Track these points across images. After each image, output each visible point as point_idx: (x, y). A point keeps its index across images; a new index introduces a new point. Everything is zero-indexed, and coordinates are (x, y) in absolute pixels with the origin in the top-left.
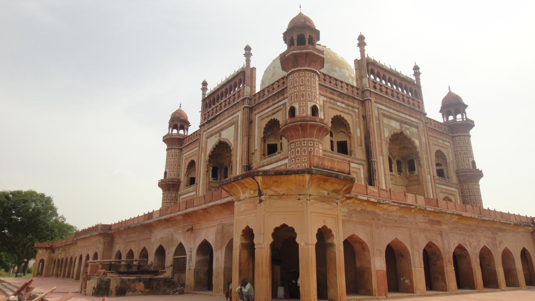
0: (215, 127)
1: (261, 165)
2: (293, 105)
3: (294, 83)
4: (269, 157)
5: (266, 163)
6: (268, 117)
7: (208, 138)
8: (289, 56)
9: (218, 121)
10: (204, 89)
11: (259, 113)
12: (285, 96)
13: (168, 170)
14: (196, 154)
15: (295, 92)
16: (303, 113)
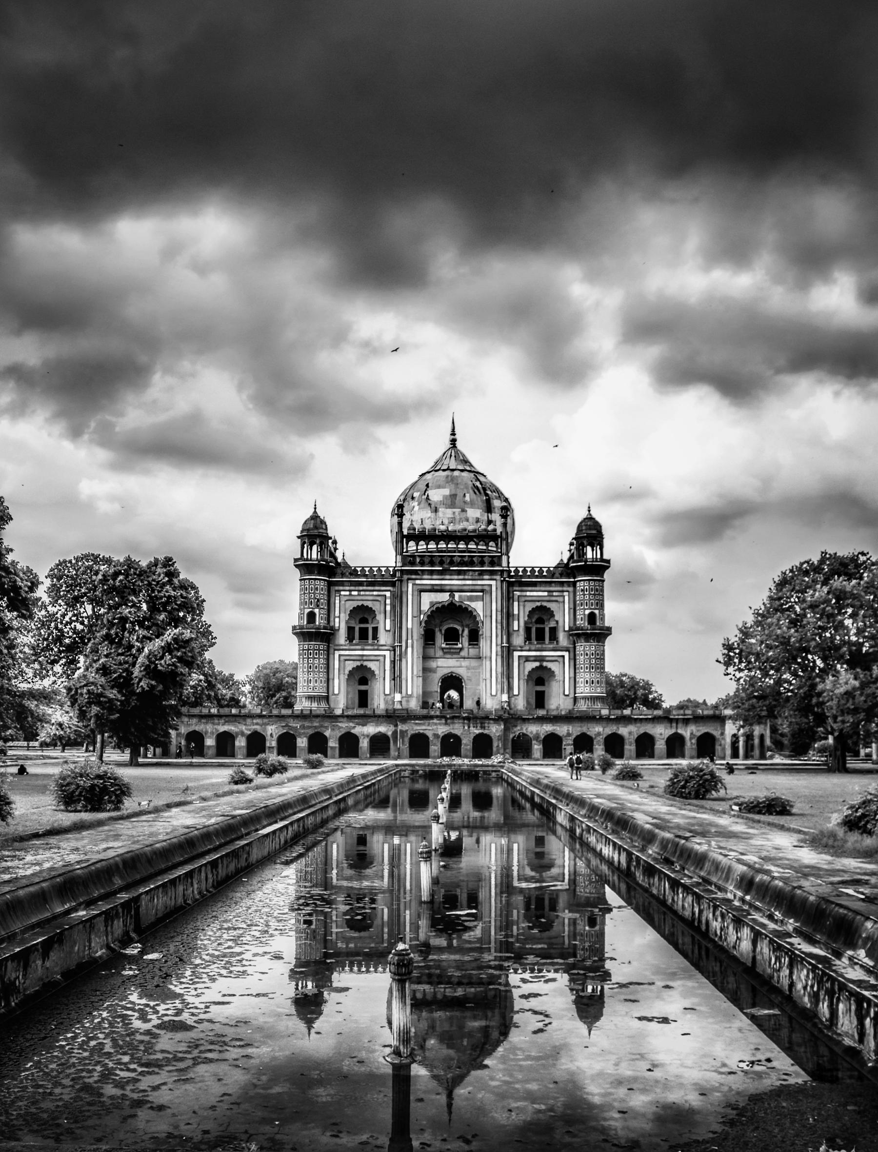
9: (448, 577)
13: (317, 611)
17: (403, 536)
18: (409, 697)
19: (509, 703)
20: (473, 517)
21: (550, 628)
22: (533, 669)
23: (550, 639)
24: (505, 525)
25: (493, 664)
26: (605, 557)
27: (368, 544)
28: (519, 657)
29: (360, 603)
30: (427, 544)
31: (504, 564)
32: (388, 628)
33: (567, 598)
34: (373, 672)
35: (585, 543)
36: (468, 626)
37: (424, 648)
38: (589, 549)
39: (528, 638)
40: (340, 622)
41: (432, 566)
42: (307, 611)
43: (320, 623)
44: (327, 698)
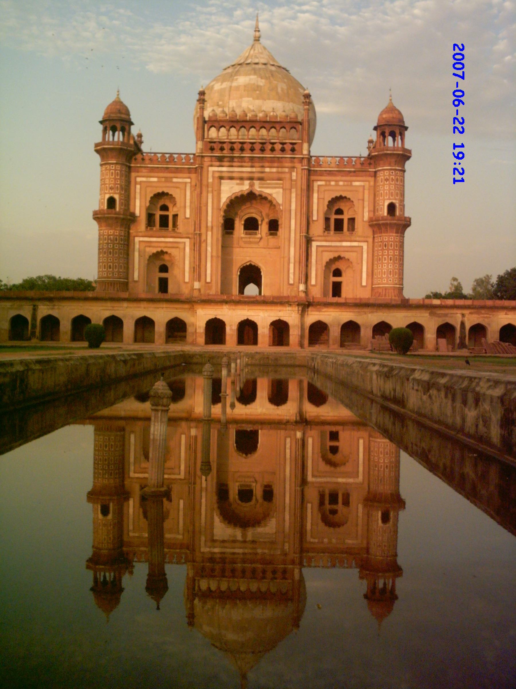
2: (394, 201)
7: (221, 178)
13: (117, 197)
17: (205, 122)
19: (306, 292)
20: (276, 107)
21: (349, 219)
23: (348, 230)
25: (293, 252)
26: (407, 146)
28: (317, 246)
31: (305, 152)
32: (188, 215)
36: (268, 215)
37: (223, 236)
38: (390, 139)
39: (327, 228)
41: (233, 154)
42: (107, 196)
43: (120, 209)
44: (127, 284)
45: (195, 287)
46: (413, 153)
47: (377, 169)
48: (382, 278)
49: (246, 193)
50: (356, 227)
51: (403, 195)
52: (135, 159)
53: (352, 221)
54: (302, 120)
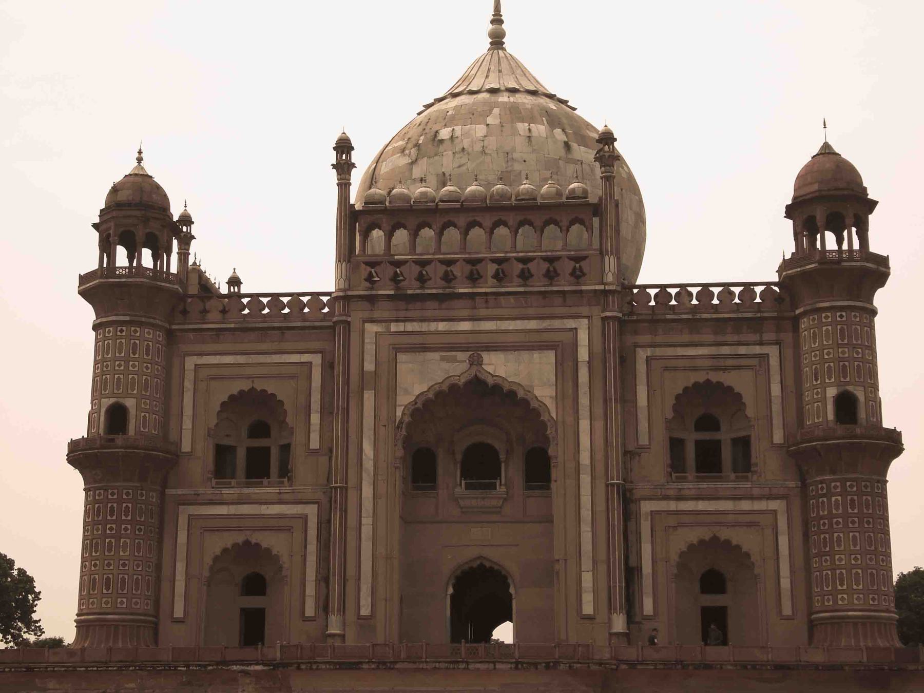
0: (442, 326)
1: (671, 493)
2: (850, 388)
3: (850, 337)
4: (700, 479)
5: (693, 492)
6: (695, 369)
7: (398, 349)
8: (852, 269)
10: (344, 168)
11: (653, 345)
12: (769, 336)
13: (130, 403)
14: (292, 377)
15: (856, 359)
16: (873, 417)
18: (365, 624)
21: (735, 441)
22: (691, 547)
23: (735, 470)
24: (608, 179)
27: (270, 241)
29: (245, 386)
30: (415, 234)
31: (610, 278)
32: (315, 444)
33: (774, 362)
34: (277, 558)
35: (820, 214)
39: (676, 465)
40: (192, 434)
42: (107, 402)
45: (331, 631)
46: (892, 263)
47: (797, 312)
48: (834, 593)
49: (463, 380)
50: (753, 460)
51: (872, 374)
52: (185, 312)
53: (743, 444)
54: (600, 199)
